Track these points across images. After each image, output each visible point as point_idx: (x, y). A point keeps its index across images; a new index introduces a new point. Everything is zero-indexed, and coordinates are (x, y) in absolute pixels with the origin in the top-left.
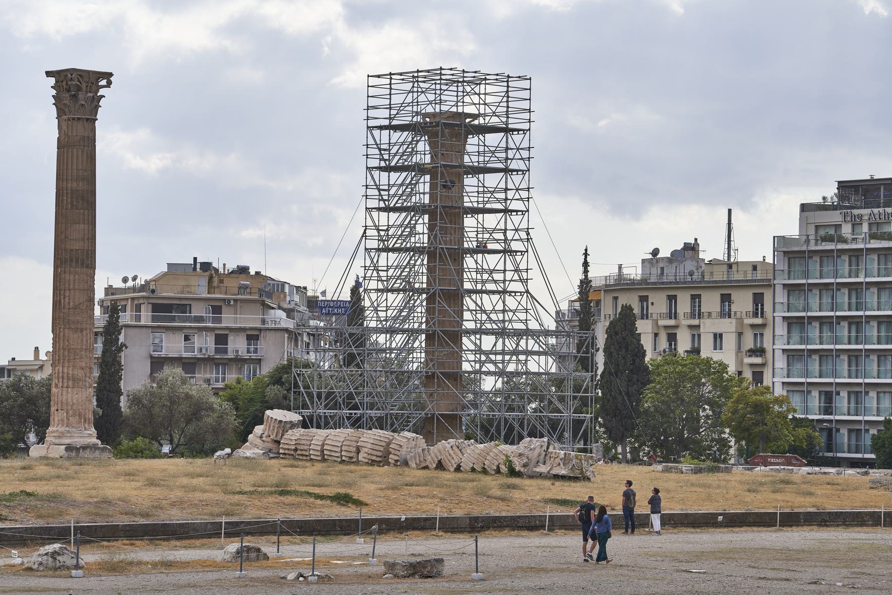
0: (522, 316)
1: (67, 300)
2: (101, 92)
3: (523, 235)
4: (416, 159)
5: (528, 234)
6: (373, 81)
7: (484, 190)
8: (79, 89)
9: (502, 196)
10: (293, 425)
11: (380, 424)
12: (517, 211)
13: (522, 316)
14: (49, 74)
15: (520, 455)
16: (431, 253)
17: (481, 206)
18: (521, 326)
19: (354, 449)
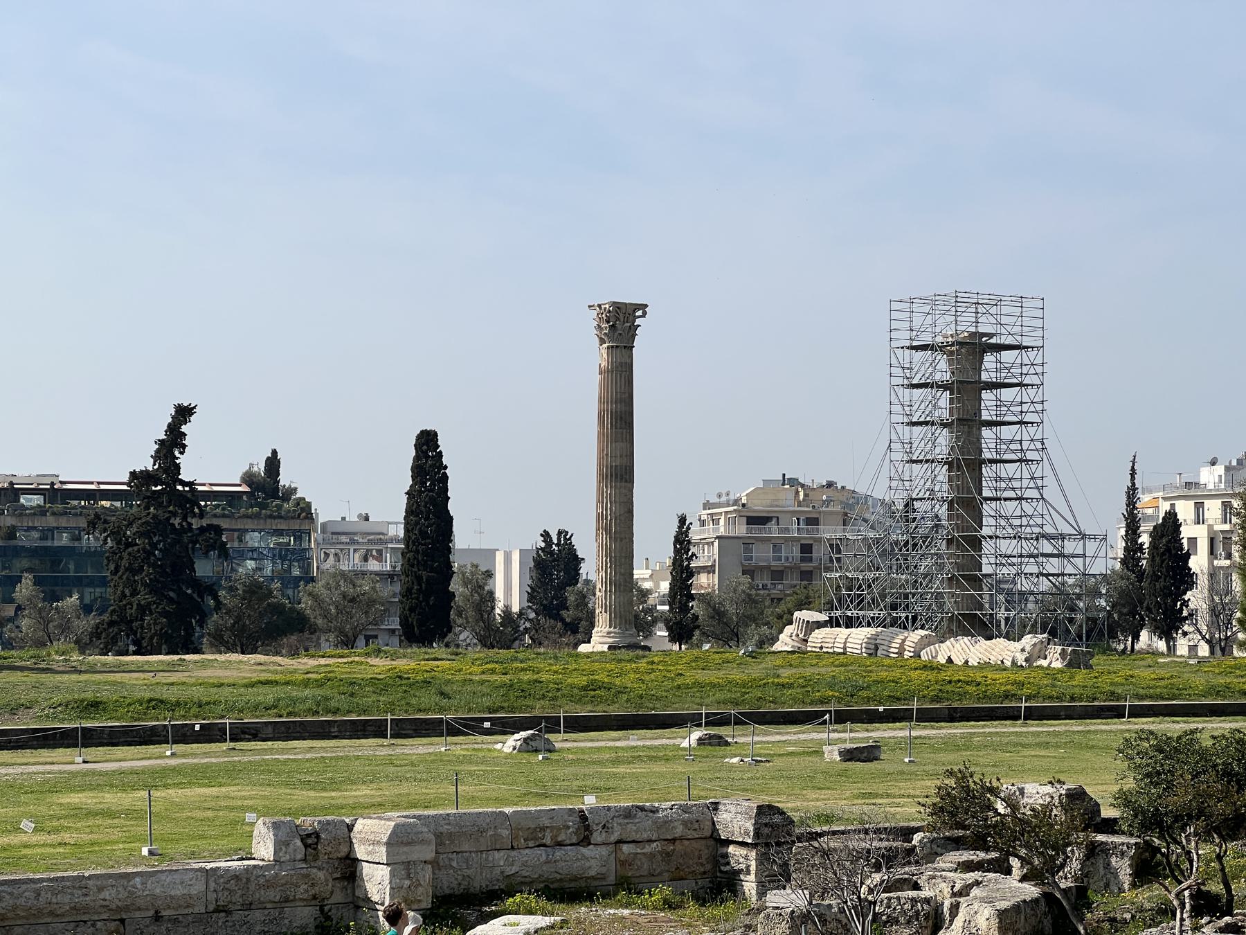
0: (1039, 521)
2: (638, 322)
3: (1039, 446)
4: (938, 377)
5: (1043, 444)
6: (895, 306)
7: (1000, 403)
10: (819, 625)
12: (1032, 423)
13: (1039, 521)
17: (998, 418)
18: (1037, 530)
19: (873, 647)
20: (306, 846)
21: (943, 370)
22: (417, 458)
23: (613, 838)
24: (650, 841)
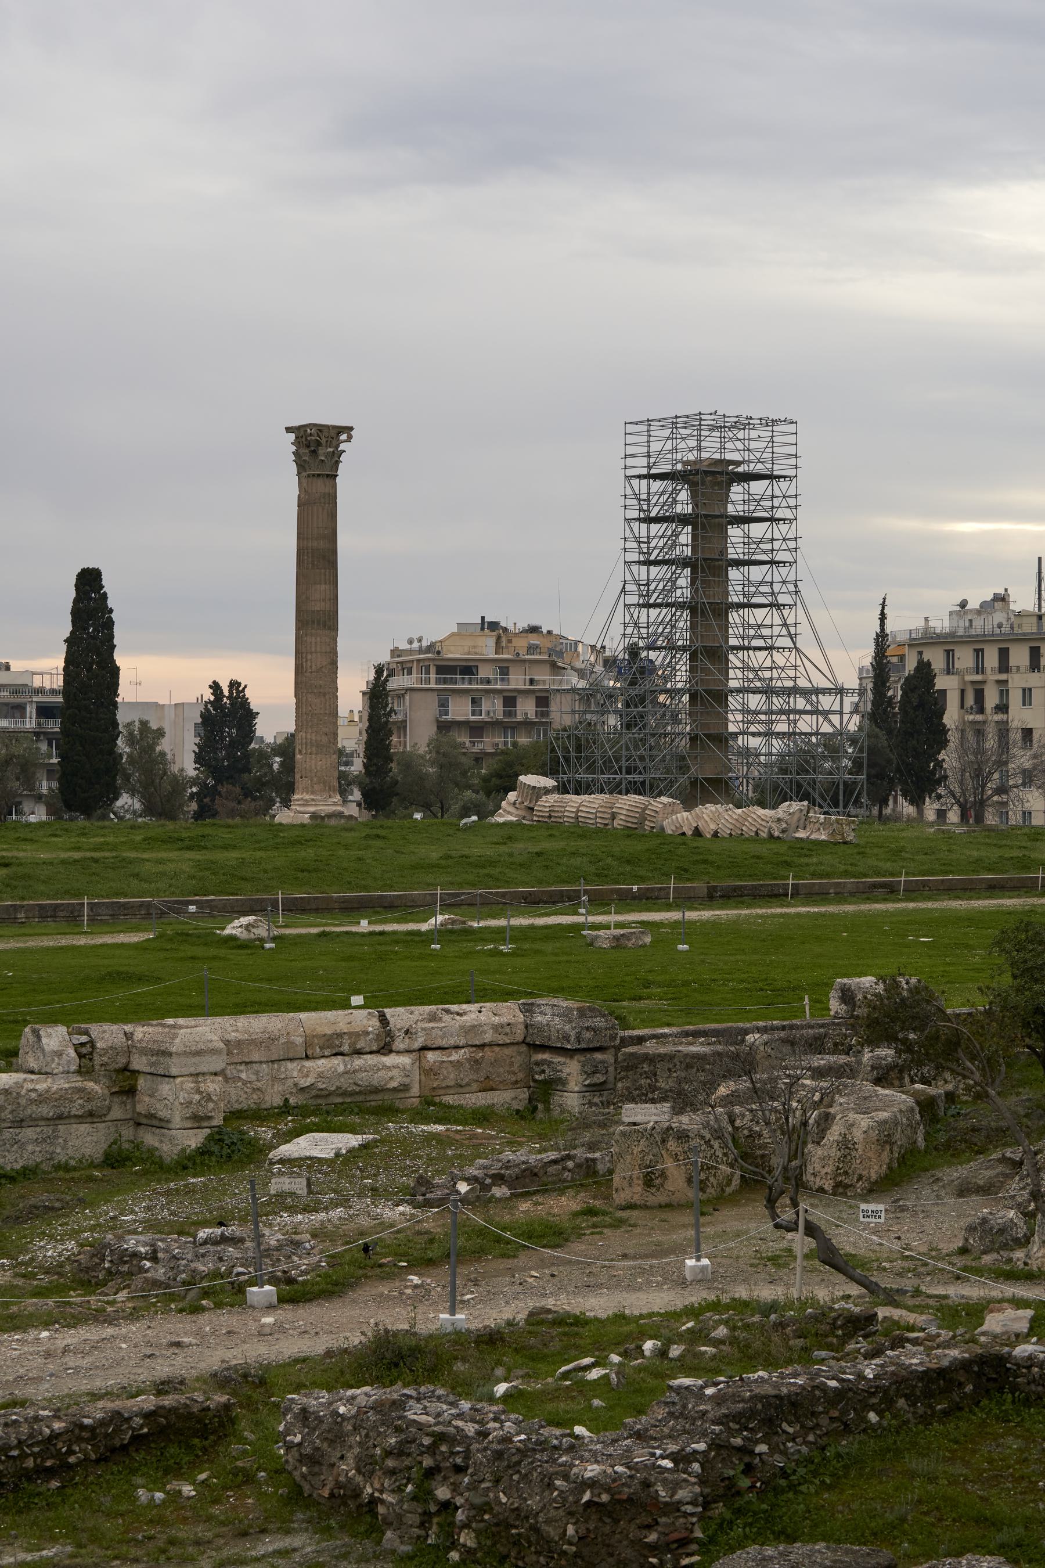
0: (792, 673)
1: (309, 664)
2: (342, 447)
3: (792, 588)
4: (679, 509)
5: (796, 586)
6: (631, 428)
7: (748, 540)
8: (319, 444)
9: (769, 546)
10: (547, 791)
11: (638, 788)
12: (784, 563)
14: (289, 430)
15: (779, 820)
16: (693, 608)
17: (746, 557)
18: (789, 684)
19: (609, 816)
20: (81, 1056)
21: (684, 502)
22: (76, 601)
23: (417, 1045)
24: (457, 1047)
